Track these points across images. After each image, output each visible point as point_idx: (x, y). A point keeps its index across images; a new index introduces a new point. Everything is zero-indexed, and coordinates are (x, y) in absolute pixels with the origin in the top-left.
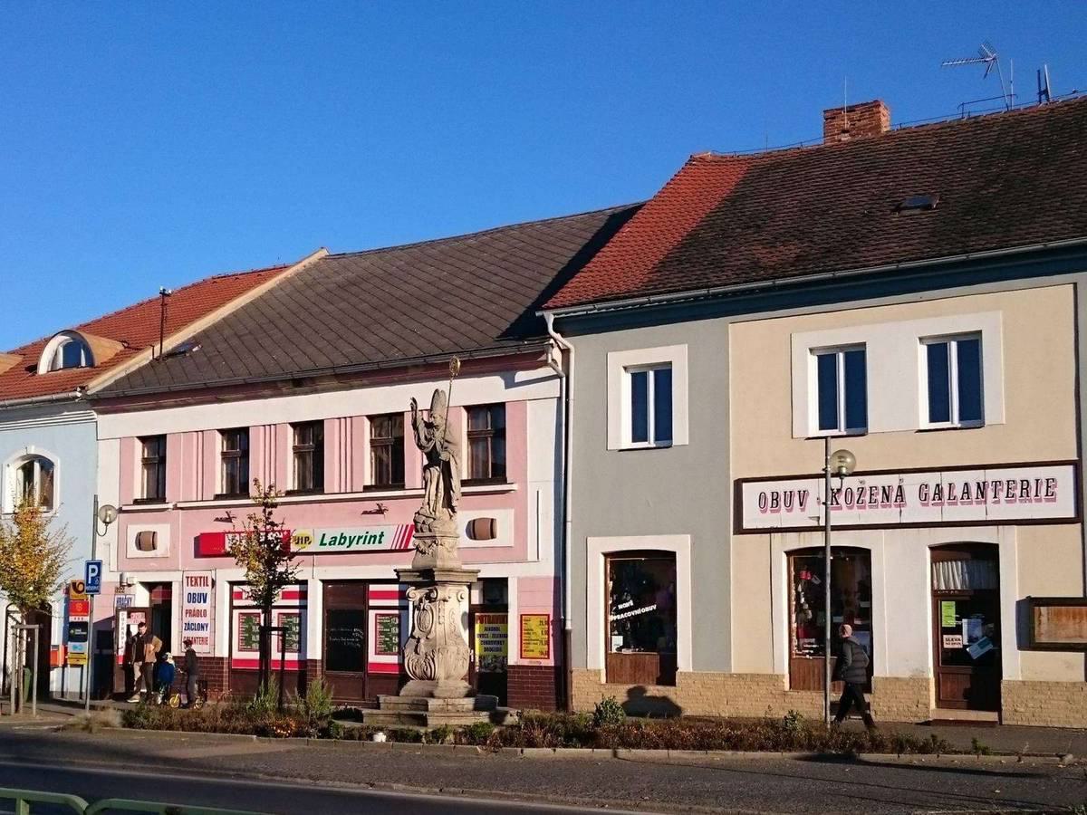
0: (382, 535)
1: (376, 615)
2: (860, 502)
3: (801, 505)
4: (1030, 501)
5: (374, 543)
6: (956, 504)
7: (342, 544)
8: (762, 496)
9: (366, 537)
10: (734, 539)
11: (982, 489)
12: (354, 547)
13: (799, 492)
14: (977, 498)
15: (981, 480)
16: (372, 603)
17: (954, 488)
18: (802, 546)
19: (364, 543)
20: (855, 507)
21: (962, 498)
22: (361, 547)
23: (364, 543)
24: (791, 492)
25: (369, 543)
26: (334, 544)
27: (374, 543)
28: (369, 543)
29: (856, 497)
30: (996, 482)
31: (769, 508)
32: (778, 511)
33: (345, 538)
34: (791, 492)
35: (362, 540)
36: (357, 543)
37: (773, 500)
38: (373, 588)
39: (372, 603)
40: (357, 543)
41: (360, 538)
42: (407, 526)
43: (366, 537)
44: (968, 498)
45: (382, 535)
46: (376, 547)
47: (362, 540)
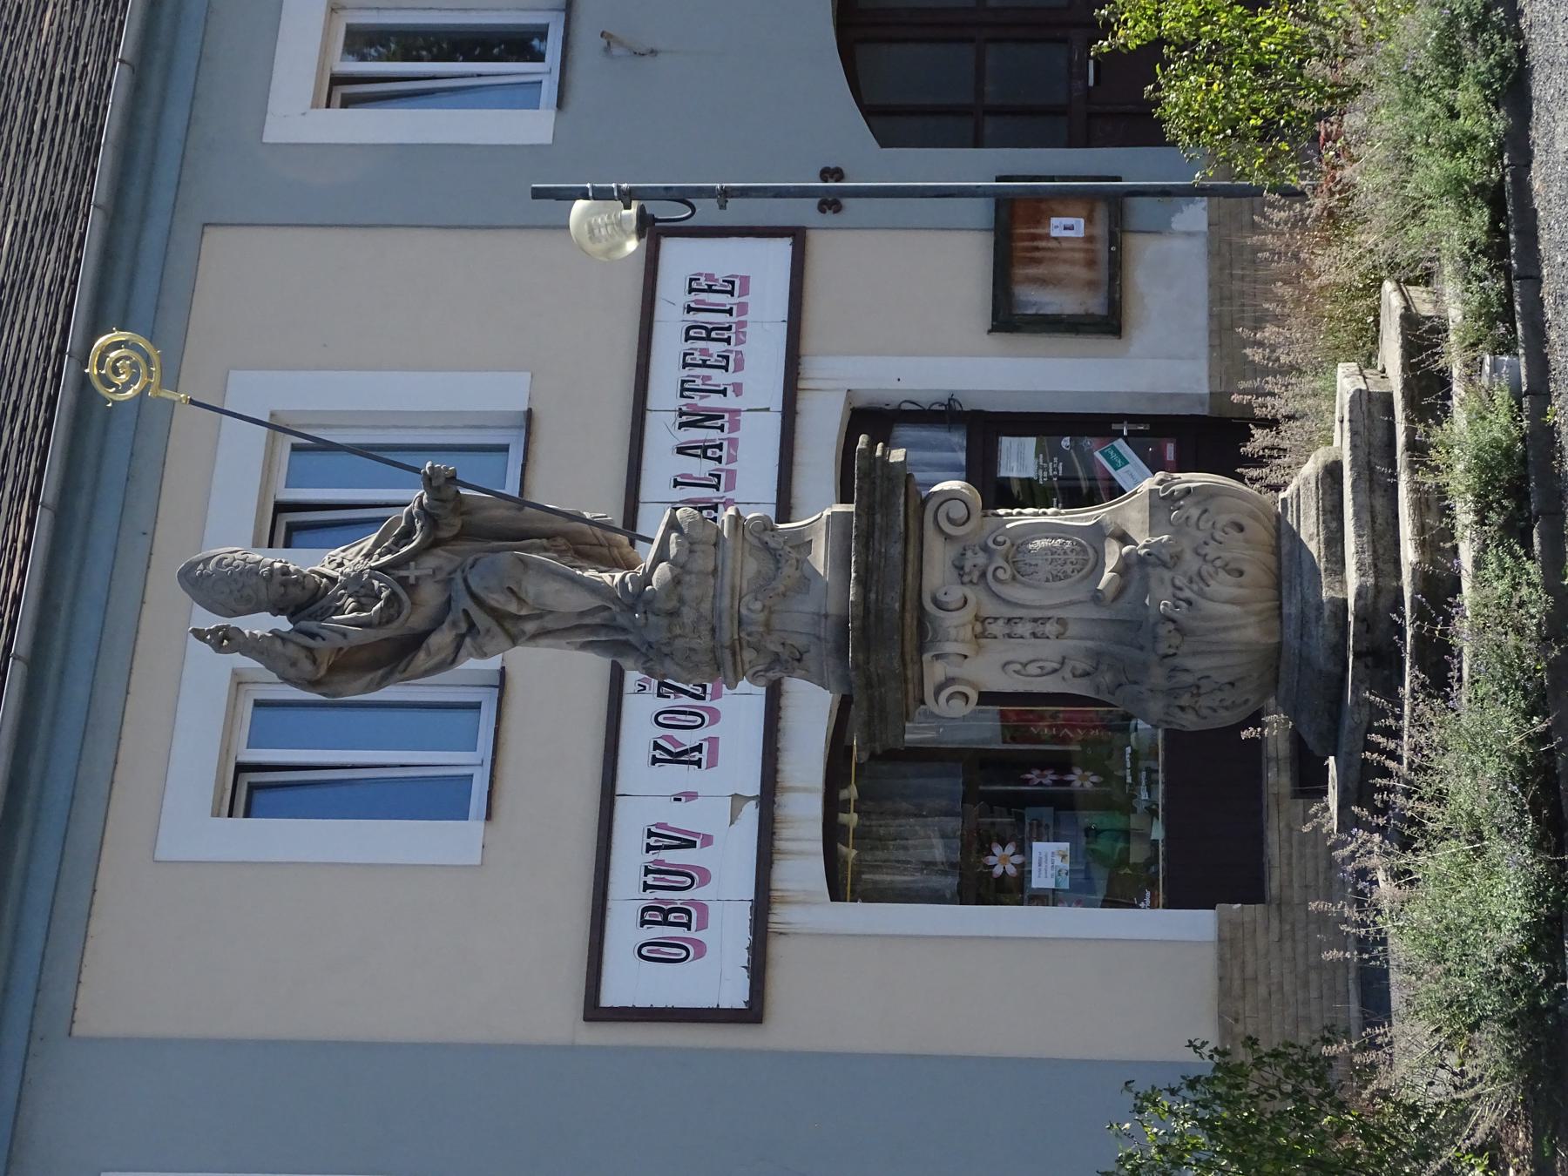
2: (699, 691)
3: (692, 844)
4: (742, 324)
6: (732, 474)
8: (650, 953)
10: (771, 1036)
11: (695, 419)
13: (649, 848)
14: (722, 428)
15: (672, 418)
17: (690, 476)
18: (819, 847)
20: (715, 704)
21: (719, 459)
24: (648, 871)
29: (685, 700)
30: (683, 389)
31: (692, 934)
32: (703, 908)
34: (648, 871)
37: (665, 922)
44: (720, 447)
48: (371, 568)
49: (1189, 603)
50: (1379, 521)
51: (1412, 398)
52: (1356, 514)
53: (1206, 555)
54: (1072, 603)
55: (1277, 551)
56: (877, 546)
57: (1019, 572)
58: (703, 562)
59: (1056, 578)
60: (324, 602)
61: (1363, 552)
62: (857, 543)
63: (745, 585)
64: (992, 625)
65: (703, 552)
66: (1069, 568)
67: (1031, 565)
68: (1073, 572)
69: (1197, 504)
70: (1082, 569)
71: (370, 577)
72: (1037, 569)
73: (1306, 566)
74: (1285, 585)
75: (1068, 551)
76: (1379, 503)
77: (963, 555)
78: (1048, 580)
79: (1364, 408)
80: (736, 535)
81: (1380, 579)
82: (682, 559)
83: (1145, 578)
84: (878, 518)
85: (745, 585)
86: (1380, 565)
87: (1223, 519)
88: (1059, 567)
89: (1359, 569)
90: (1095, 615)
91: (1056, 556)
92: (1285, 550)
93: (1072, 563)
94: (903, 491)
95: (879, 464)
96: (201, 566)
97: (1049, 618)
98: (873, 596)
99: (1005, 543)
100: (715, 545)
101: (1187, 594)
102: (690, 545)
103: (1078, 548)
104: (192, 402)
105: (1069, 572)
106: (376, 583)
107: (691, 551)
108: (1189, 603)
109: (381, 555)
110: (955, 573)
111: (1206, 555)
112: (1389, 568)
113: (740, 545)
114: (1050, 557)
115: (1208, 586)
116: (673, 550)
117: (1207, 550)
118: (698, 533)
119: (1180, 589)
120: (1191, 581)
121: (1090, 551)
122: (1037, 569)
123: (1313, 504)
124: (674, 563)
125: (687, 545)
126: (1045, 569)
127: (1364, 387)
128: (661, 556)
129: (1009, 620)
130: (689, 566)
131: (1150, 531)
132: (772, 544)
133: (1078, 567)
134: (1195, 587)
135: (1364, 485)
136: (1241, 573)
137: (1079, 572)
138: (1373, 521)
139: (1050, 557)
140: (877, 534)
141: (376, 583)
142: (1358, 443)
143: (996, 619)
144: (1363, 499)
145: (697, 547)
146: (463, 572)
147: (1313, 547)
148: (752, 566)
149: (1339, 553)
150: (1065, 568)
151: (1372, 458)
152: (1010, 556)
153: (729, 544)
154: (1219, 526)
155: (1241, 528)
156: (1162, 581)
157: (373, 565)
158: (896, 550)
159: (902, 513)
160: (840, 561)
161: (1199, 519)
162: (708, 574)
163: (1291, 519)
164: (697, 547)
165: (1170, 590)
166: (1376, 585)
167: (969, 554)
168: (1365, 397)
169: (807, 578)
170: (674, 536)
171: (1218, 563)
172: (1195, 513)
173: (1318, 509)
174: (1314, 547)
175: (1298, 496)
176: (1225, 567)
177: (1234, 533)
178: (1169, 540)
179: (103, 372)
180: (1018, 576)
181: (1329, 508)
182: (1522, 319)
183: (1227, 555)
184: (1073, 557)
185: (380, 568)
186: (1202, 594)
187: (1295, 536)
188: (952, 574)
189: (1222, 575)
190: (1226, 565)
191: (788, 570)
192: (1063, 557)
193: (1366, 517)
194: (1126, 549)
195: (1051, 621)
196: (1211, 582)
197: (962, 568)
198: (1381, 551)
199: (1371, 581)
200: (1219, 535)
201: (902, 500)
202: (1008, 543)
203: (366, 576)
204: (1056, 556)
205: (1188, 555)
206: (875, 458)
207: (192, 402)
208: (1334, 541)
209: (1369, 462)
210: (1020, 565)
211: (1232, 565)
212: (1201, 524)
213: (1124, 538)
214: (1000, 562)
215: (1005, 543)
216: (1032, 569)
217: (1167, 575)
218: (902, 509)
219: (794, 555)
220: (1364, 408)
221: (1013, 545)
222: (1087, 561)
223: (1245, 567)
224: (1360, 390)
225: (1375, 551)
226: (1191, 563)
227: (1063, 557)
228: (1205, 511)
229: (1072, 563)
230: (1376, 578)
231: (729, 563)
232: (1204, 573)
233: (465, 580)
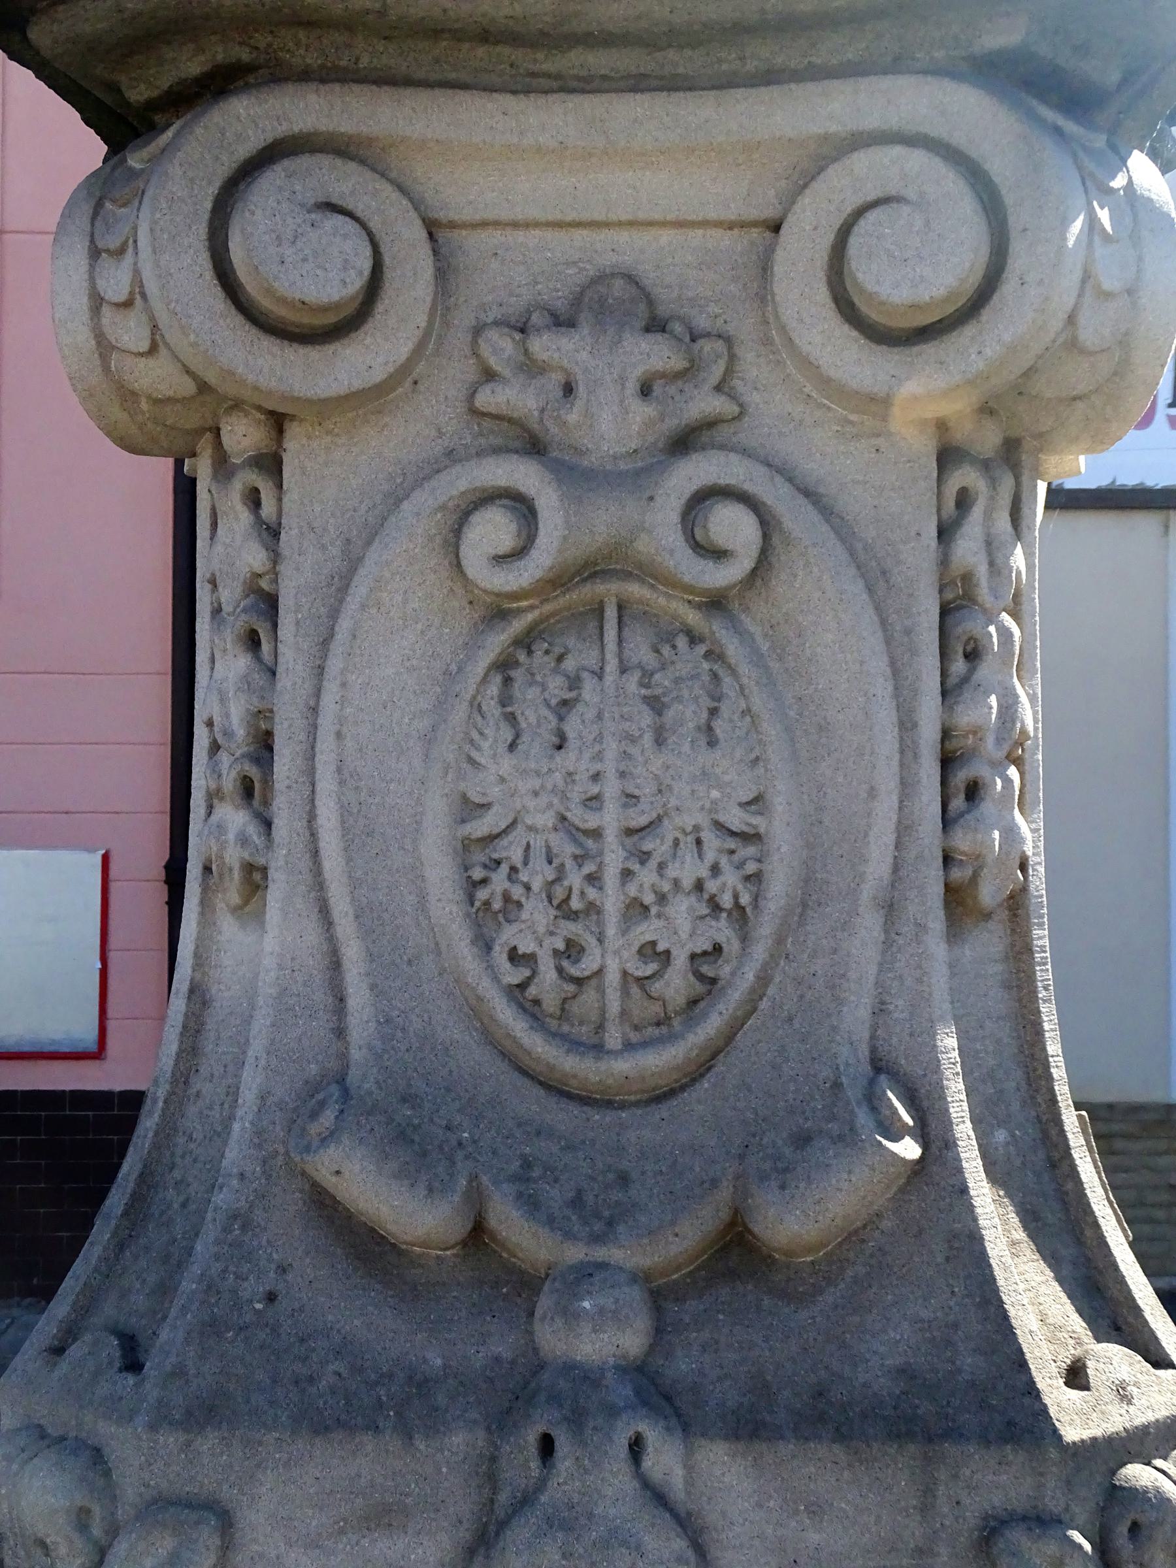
54: (335, 965)
57: (525, 642)
64: (245, 516)
67: (565, 706)
68: (514, 956)
70: (531, 1009)
72: (535, 746)
75: (646, 931)
77: (656, 325)
78: (470, 808)
88: (538, 874)
90: (248, 1097)
91: (614, 858)
93: (572, 950)
97: (267, 825)
99: (719, 554)
105: (509, 935)
110: (557, 293)
114: (610, 819)
122: (535, 746)
129: (269, 604)
139: (610, 819)
143: (271, 533)
150: (537, 913)
152: (635, 590)
180: (498, 641)
192: (612, 902)
195: (253, 831)
197: (563, 322)
204: (614, 858)
210: (581, 656)
215: (719, 554)
222: (598, 1049)
227: (612, 902)
229: (572, 950)
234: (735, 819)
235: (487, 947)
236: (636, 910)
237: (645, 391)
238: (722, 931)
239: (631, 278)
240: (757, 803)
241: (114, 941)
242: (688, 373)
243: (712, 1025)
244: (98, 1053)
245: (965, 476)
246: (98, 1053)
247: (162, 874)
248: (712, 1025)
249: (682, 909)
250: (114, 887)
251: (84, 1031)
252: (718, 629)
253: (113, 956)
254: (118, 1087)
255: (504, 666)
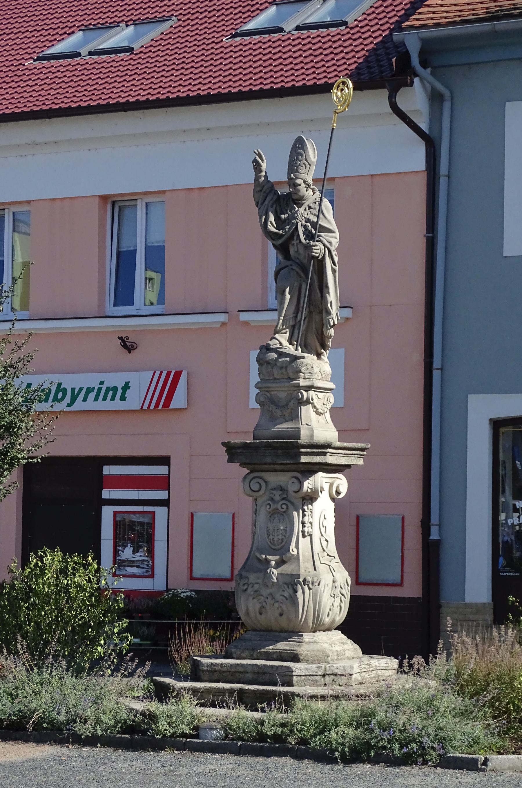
0: (126, 386)
1: (115, 513)
5: (113, 399)
7: (59, 401)
9: (100, 389)
12: (79, 405)
16: (106, 494)
19: (96, 399)
22: (91, 405)
23: (96, 399)
25: (104, 399)
26: (46, 400)
27: (113, 399)
28: (104, 399)
33: (65, 391)
35: (92, 395)
36: (85, 399)
38: (108, 470)
39: (106, 494)
40: (85, 399)
41: (89, 390)
42: (169, 374)
43: (100, 389)
45: (126, 386)
46: (118, 405)
47: (92, 395)
48: (297, 223)
49: (246, 590)
50: (241, 675)
51: (264, 694)
52: (242, 665)
53: (267, 598)
55: (282, 631)
56: (267, 451)
58: (276, 373)
59: (268, 531)
60: (292, 203)
61: (222, 667)
62: (266, 442)
63: (273, 393)
65: (282, 373)
66: (271, 537)
69: (290, 596)
71: (293, 223)
73: (265, 643)
74: (266, 633)
76: (250, 676)
77: (281, 490)
79: (287, 673)
80: (292, 387)
81: (207, 673)
82: (278, 364)
83: (259, 571)
84: (280, 451)
85: (273, 393)
86: (215, 673)
87: (284, 608)
89: (212, 664)
92: (281, 634)
94: (291, 462)
95: (297, 450)
96: (300, 146)
98: (239, 451)
100: (289, 378)
101: (250, 590)
102: (284, 367)
103: (280, 541)
104: (333, 129)
105: (270, 537)
106: (288, 227)
107: (282, 367)
108: (246, 590)
109: (305, 227)
111: (267, 598)
112: (215, 676)
113: (290, 389)
114: (276, 529)
115: (253, 599)
116: (280, 360)
117: (269, 601)
118: (289, 370)
119: (253, 586)
120: (256, 591)
121: (280, 547)
123: (288, 648)
124: (277, 359)
125: (284, 365)
126: (271, 526)
127: (294, 674)
128: (281, 355)
130: (275, 368)
131: (281, 574)
132: (291, 404)
133: (272, 541)
134: (252, 593)
135: (256, 670)
136: (261, 614)
137: (270, 542)
138: (240, 672)
139: (276, 529)
140: (273, 451)
141: (288, 227)
142: (274, 669)
144: (249, 669)
145: (284, 370)
146: (291, 265)
147: (271, 647)
148: (282, 395)
149: (261, 657)
150: (271, 536)
151: (268, 675)
153: (287, 384)
154: (281, 605)
155: (281, 615)
156: (258, 578)
157: (299, 224)
158: (268, 460)
159: (282, 462)
160: (279, 436)
161: (284, 596)
162: (273, 375)
163: (295, 638)
164: (284, 370)
165: (253, 582)
166: (203, 671)
167: (280, 493)
168: (290, 673)
169: (274, 420)
170: (288, 359)
171: (264, 604)
172: (286, 594)
173: (284, 650)
174: (270, 648)
175: (299, 642)
176: (263, 607)
177: (278, 612)
178: (273, 583)
179: (341, 85)
181: (283, 655)
182: (202, 742)
183: (268, 607)
184: (276, 539)
185: (297, 228)
186: (250, 595)
187: (285, 639)
188: (272, 485)
189: (258, 606)
190: (264, 607)
191: (278, 413)
193: (241, 670)
194: (273, 563)
196: (255, 600)
198: (224, 674)
199: (205, 669)
200: (276, 605)
201: (288, 462)
202: (284, 510)
203: (293, 221)
205: (269, 591)
206: (299, 449)
207: (333, 129)
208: (268, 656)
209: (267, 673)
211: (263, 610)
212: (282, 597)
213: (280, 563)
214: (273, 507)
216: (271, 520)
217: (260, 581)
218: (285, 462)
219: (287, 415)
220: (287, 673)
221: (284, 512)
222: (275, 545)
223: (263, 616)
224: (292, 672)
225: (224, 672)
226: (265, 592)
228: (287, 599)
229: (273, 538)
230: (208, 671)
231: (277, 385)
232: (260, 597)
233: (287, 266)
234: (285, 529)
235: (268, 538)
236: (277, 536)
237: (280, 495)
238: (283, 537)
239: (281, 486)
240: (286, 527)
241: (406, 547)
242: (283, 494)
243: (282, 544)
244: (400, 584)
245: (304, 501)
246: (400, 584)
247: (420, 523)
248: (282, 544)
249: (281, 536)
250: (406, 529)
251: (395, 577)
252: (284, 514)
253: (406, 552)
254: (407, 597)
255: (270, 517)
